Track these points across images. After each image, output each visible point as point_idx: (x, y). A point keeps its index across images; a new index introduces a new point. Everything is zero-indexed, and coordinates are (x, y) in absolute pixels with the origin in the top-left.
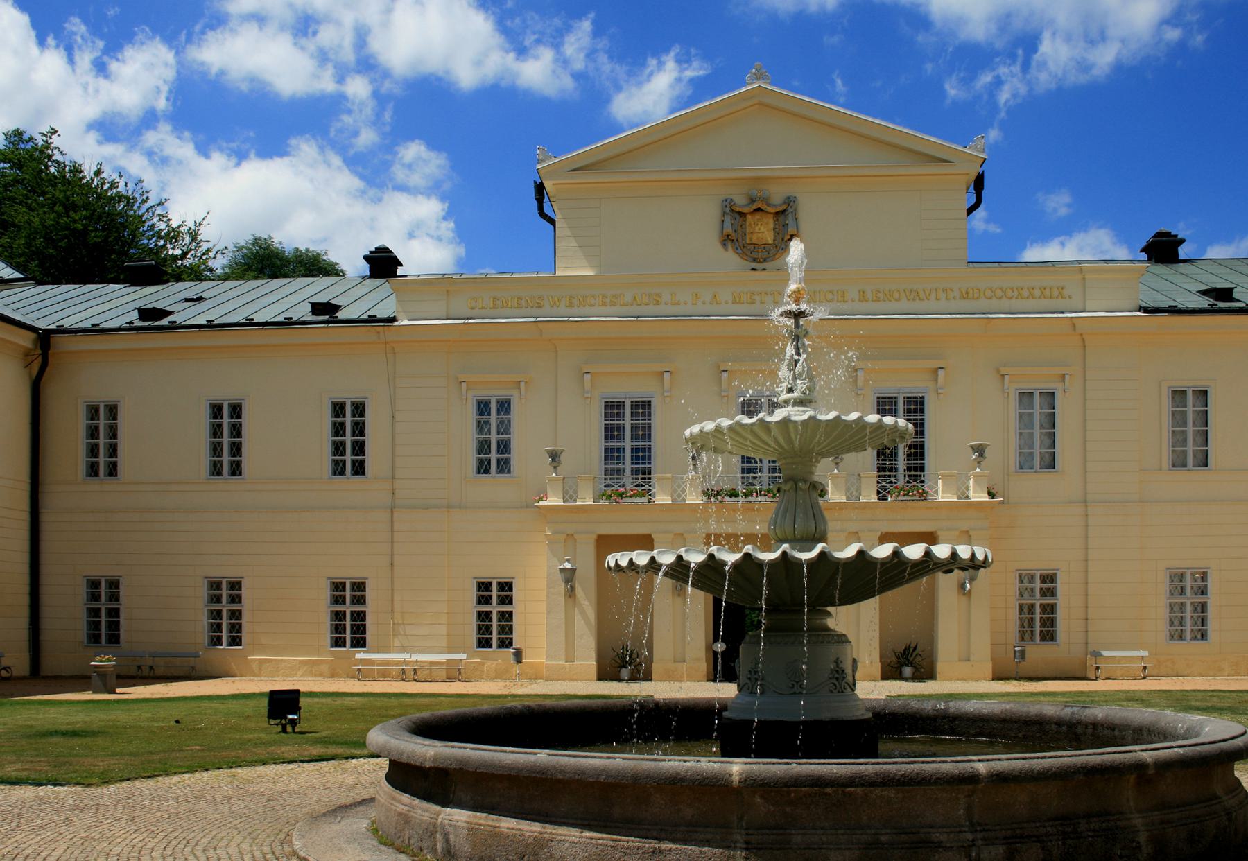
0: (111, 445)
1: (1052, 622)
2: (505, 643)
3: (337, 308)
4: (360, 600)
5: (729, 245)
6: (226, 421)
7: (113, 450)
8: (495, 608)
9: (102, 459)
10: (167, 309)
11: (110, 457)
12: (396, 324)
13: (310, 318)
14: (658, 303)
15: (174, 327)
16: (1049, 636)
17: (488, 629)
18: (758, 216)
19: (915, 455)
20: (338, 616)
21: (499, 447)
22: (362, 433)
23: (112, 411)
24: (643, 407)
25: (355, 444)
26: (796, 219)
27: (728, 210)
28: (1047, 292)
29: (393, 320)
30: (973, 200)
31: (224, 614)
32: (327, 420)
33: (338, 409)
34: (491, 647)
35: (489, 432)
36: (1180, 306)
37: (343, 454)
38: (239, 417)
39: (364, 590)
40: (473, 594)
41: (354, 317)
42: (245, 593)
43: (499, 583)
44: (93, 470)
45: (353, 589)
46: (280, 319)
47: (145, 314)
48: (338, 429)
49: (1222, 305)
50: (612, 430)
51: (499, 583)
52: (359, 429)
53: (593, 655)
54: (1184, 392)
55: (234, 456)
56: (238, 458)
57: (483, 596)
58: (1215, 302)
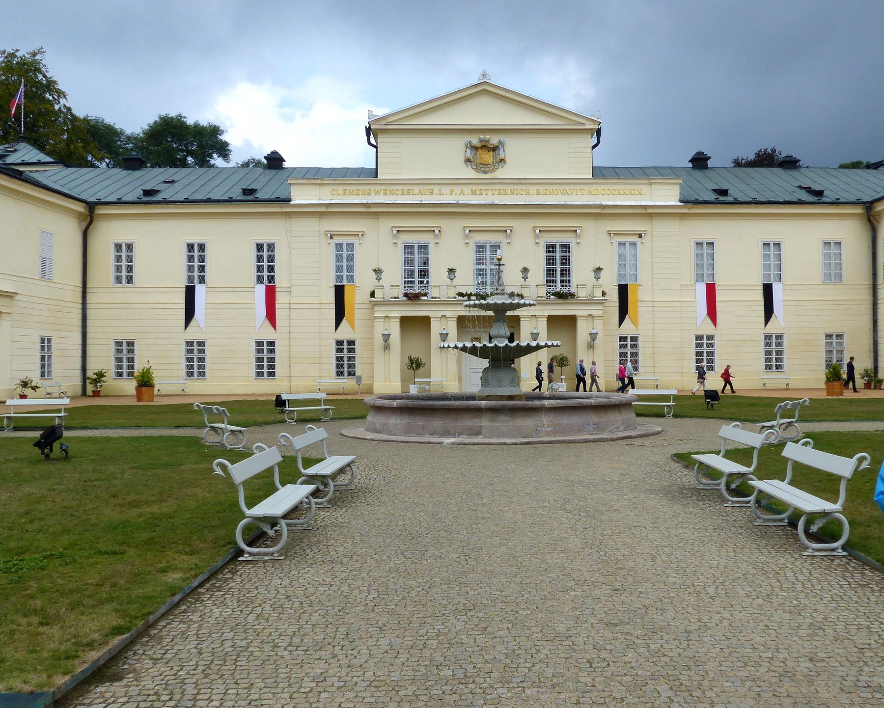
2: (352, 374)
3: (255, 190)
5: (469, 164)
6: (196, 254)
7: (130, 269)
8: (345, 355)
13: (242, 197)
14: (431, 194)
19: (566, 274)
20: (259, 360)
21: (347, 269)
22: (272, 261)
23: (130, 247)
25: (269, 266)
27: (469, 146)
30: (596, 142)
31: (195, 360)
32: (254, 252)
34: (344, 376)
36: (701, 199)
37: (262, 271)
38: (203, 251)
41: (267, 197)
42: (207, 348)
43: (348, 342)
44: (119, 280)
45: (268, 345)
47: (147, 193)
48: (260, 259)
49: (722, 198)
57: (339, 349)
58: (719, 197)
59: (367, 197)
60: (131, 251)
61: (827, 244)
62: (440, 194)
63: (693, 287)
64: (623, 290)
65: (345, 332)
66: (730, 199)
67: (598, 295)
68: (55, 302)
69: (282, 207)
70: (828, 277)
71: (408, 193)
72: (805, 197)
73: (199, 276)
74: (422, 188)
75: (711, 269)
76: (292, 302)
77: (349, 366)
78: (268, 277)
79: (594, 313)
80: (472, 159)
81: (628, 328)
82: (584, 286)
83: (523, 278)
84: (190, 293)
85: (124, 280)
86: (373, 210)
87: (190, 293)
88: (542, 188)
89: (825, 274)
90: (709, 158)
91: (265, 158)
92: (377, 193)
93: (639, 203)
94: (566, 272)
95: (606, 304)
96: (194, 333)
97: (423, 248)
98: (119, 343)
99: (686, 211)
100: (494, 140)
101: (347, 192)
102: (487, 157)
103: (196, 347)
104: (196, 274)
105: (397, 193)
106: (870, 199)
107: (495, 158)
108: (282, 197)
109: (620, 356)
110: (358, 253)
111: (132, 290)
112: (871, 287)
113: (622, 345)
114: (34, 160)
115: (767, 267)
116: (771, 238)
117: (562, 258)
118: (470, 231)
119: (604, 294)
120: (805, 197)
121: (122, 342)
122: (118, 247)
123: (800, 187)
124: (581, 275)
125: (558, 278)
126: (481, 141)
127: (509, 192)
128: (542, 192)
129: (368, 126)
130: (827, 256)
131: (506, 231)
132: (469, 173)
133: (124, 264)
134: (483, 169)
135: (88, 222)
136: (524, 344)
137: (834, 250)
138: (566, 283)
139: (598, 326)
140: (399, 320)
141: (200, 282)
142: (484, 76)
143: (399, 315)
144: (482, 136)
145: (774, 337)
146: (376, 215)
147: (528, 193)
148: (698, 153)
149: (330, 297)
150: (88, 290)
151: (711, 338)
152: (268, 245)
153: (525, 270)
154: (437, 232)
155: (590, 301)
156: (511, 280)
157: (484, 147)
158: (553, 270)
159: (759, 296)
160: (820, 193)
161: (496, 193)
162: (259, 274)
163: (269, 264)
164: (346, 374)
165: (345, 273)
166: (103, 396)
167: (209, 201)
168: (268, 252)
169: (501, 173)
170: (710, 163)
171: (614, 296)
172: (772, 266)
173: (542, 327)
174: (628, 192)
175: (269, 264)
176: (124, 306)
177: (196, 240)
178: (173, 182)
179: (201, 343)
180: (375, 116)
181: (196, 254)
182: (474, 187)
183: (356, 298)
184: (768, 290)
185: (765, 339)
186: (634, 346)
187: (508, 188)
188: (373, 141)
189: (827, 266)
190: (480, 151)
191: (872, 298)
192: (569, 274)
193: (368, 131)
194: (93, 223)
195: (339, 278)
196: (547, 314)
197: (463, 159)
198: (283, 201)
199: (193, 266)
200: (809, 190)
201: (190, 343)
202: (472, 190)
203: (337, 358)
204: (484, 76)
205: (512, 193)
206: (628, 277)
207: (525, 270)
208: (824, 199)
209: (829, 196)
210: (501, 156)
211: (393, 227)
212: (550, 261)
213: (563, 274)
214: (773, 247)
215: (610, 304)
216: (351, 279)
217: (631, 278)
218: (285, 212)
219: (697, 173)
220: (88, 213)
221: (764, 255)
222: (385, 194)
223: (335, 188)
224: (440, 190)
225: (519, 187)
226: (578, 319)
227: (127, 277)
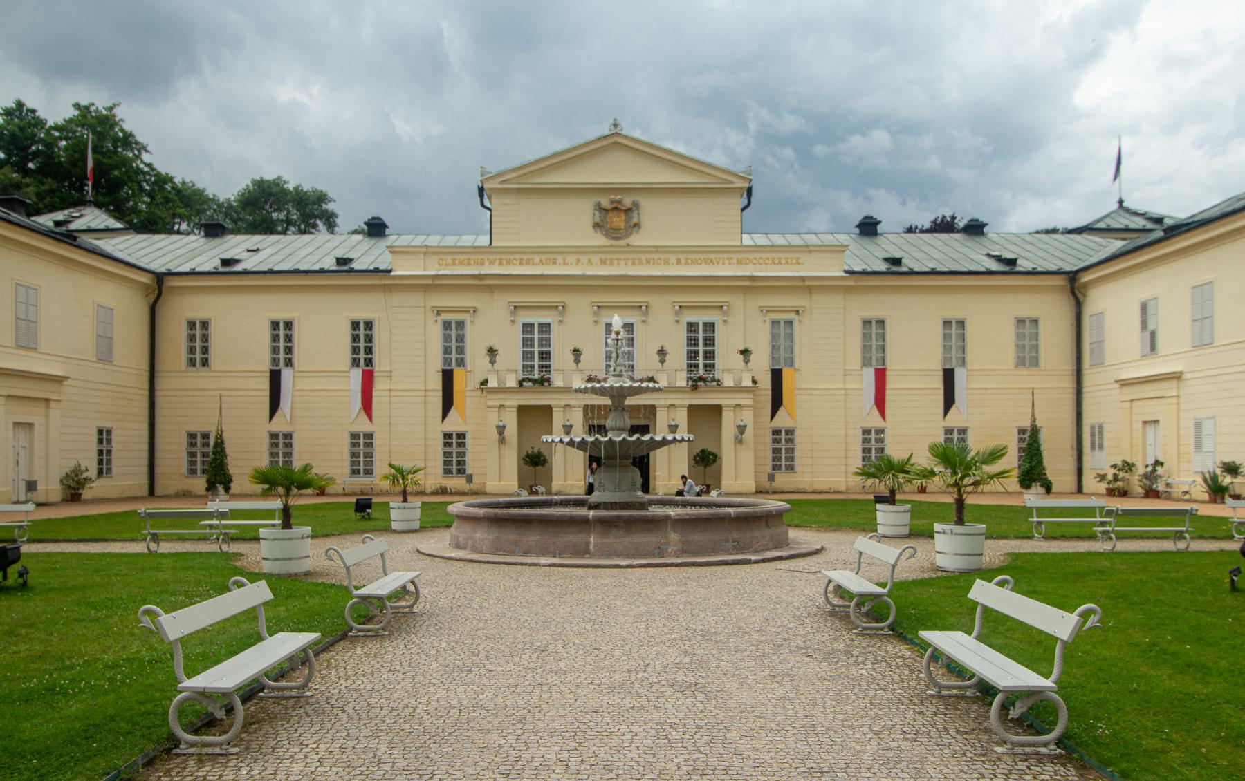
0: (204, 347)
1: (792, 459)
2: (461, 472)
4: (370, 445)
6: (282, 332)
7: (205, 350)
8: (454, 450)
9: (198, 356)
10: (237, 257)
11: (204, 354)
12: (392, 274)
13: (334, 268)
14: (554, 263)
15: (245, 273)
16: (791, 468)
17: (450, 462)
18: (615, 213)
20: (353, 455)
22: (370, 341)
23: (205, 324)
24: (546, 327)
25: (366, 348)
26: (639, 214)
28: (789, 261)
29: (390, 271)
30: (746, 202)
31: (281, 455)
32: (347, 332)
33: (355, 325)
35: (451, 341)
37: (358, 353)
38: (290, 329)
39: (372, 439)
40: (441, 441)
41: (364, 267)
42: (295, 441)
43: (457, 434)
44: (192, 362)
45: (364, 438)
46: (316, 268)
47: (226, 262)
48: (355, 338)
49: (895, 269)
50: (527, 341)
51: (457, 434)
52: (369, 339)
53: (516, 478)
54: (870, 322)
55: (287, 354)
56: (290, 356)
57: (447, 443)
59: (479, 267)
60: (207, 329)
61: (1020, 322)
62: (564, 264)
63: (860, 373)
64: (777, 376)
65: (454, 423)
66: (904, 269)
67: (747, 382)
68: (115, 388)
69: (381, 279)
70: (1021, 362)
71: (527, 263)
72: (994, 266)
73: (285, 359)
74: (544, 257)
75: (881, 351)
76: (392, 388)
77: (459, 463)
78: (365, 359)
79: (742, 402)
80: (601, 224)
81: (782, 421)
82: (730, 371)
83: (660, 361)
84: (275, 377)
85: (198, 362)
86: (486, 282)
87: (275, 377)
88: (683, 257)
89: (1018, 357)
90: (880, 222)
91: (365, 223)
92: (492, 263)
93: (796, 274)
94: (710, 355)
95: (758, 392)
96: (280, 424)
97: (545, 328)
98: (192, 436)
99: (851, 283)
100: (628, 201)
101: (457, 262)
102: (618, 221)
103: (281, 440)
104: (282, 356)
105: (515, 262)
106: (1075, 269)
107: (627, 221)
108: (382, 268)
109: (773, 452)
110: (469, 331)
111: (208, 374)
112: (1075, 373)
113: (776, 439)
114: (102, 227)
115: (947, 349)
116: (953, 315)
117: (705, 339)
118: (598, 307)
119: (754, 382)
120: (994, 266)
121: (196, 435)
122: (192, 325)
123: (989, 255)
124: (727, 358)
125: (701, 361)
126: (612, 202)
127: (644, 262)
128: (683, 262)
129: (480, 185)
130: (1020, 336)
131: (641, 307)
132: (599, 240)
133: (198, 344)
134: (614, 235)
135: (156, 295)
136: (658, 438)
137: (1028, 329)
138: (710, 367)
139: (747, 417)
140: (515, 410)
141: (287, 365)
142: (615, 125)
143: (516, 403)
144: (612, 197)
145: (956, 432)
146: (490, 289)
147: (667, 263)
148: (866, 218)
149: (436, 384)
150: (156, 374)
151: (880, 431)
152: (365, 322)
153: (662, 353)
154: (560, 308)
155: (738, 389)
156: (645, 361)
157: (616, 208)
158: (695, 352)
159: (938, 383)
160: (1012, 262)
161: (630, 262)
162: (355, 356)
163: (367, 344)
164: (454, 471)
165: (454, 356)
166: (160, 497)
167: (296, 271)
168: (365, 330)
169: (636, 239)
170: (880, 228)
171: (766, 383)
172: (954, 347)
173: (681, 418)
174: (783, 261)
175: (367, 344)
176: (198, 393)
177: (281, 316)
178: (258, 250)
179: (288, 436)
180: (489, 173)
181: (282, 332)
182: (604, 256)
183: (463, 383)
184: (949, 376)
185: (946, 434)
186: (790, 441)
187: (643, 257)
188: (487, 203)
189: (1020, 348)
190: (610, 214)
191: (1075, 386)
192: (714, 357)
193: (481, 191)
194: (163, 296)
195: (447, 361)
196: (687, 403)
197: (590, 223)
198: (383, 271)
199: (278, 347)
200: (999, 259)
201: (274, 436)
202: (601, 260)
203: (445, 453)
204: (615, 125)
205: (648, 262)
206: (782, 361)
207: (662, 353)
208: (1018, 269)
209: (1023, 265)
210: (635, 220)
211: (509, 302)
212: (692, 341)
213: (706, 357)
214: (955, 328)
215: (762, 392)
216: (461, 363)
217: (785, 362)
218: (385, 285)
219: (866, 241)
220: (156, 286)
221: (944, 335)
222: (501, 264)
223: (444, 257)
224: (564, 260)
225: (656, 256)
226: (724, 409)
227: (202, 359)
